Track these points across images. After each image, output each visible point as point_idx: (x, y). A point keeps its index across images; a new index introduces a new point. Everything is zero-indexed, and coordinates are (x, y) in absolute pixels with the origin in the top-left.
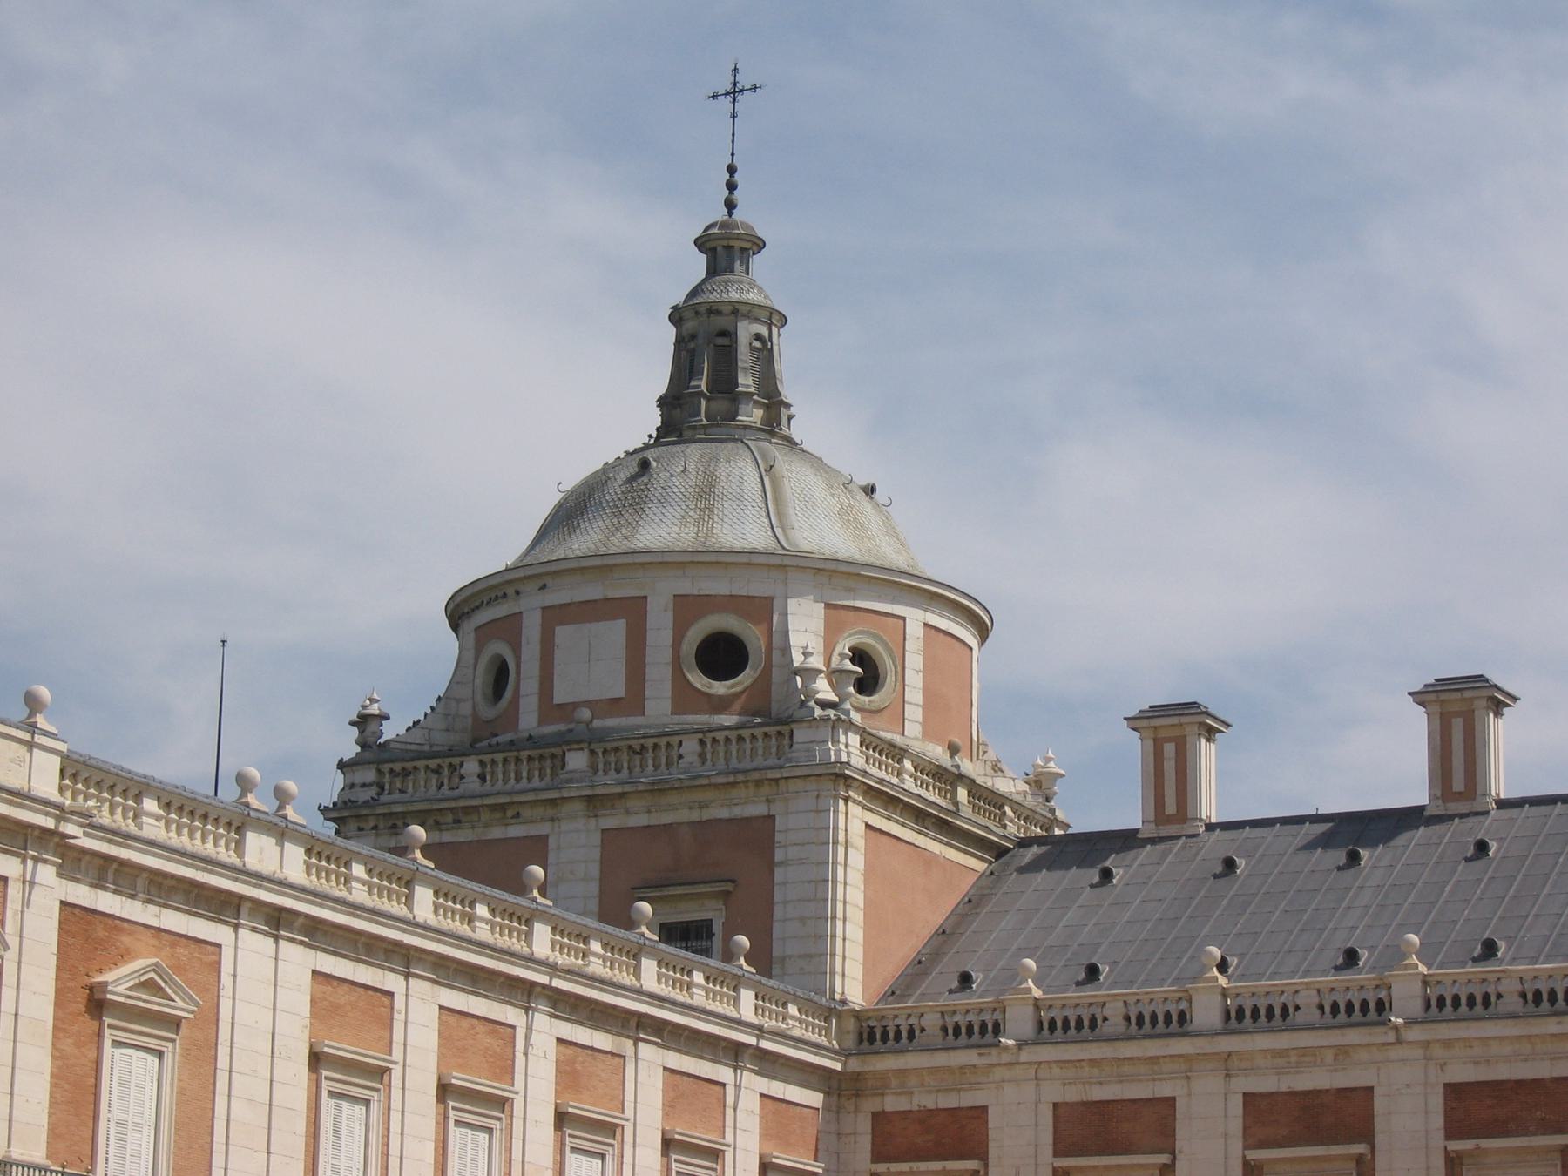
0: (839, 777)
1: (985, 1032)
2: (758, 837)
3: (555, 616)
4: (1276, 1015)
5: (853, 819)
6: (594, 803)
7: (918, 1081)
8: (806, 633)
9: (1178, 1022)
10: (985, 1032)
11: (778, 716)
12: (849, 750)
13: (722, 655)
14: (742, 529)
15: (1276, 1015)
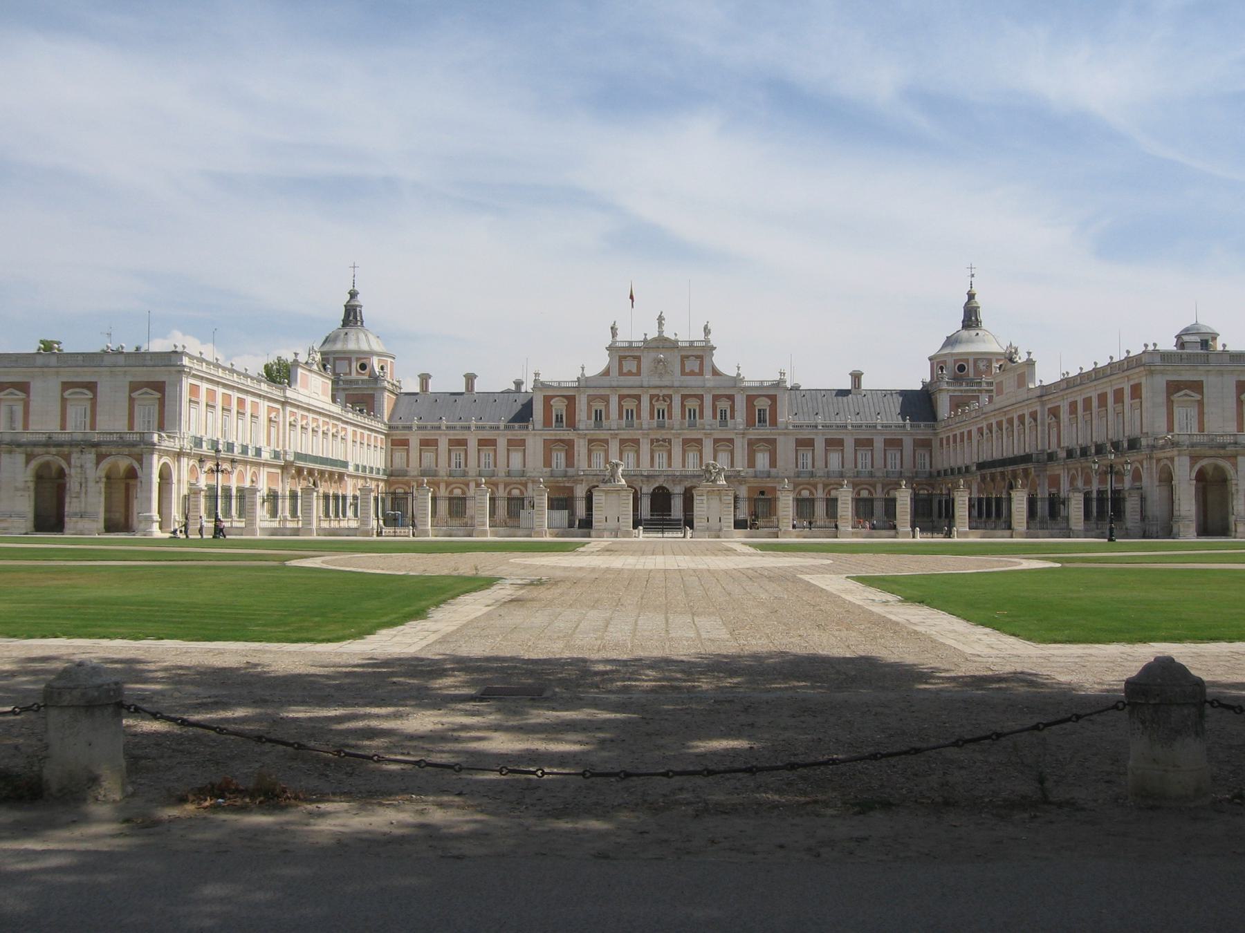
0: (385, 388)
1: (410, 428)
2: (372, 397)
3: (335, 359)
4: (453, 428)
5: (386, 394)
6: (344, 389)
7: (398, 435)
8: (375, 363)
9: (439, 428)
10: (410, 428)
11: (375, 379)
12: (386, 384)
13: (363, 367)
14: (365, 347)
15: (453, 428)
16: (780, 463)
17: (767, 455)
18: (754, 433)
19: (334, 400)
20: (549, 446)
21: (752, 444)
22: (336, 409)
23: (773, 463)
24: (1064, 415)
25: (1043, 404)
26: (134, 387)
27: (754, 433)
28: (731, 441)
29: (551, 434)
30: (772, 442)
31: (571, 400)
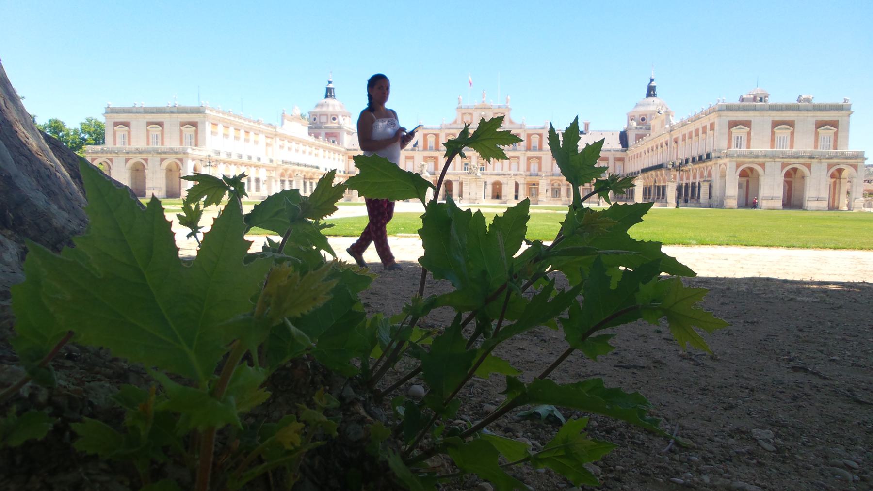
16: (543, 169)
17: (537, 165)
18: (530, 154)
19: (310, 134)
20: (426, 159)
21: (529, 158)
22: (312, 139)
23: (540, 169)
24: (680, 141)
25: (671, 136)
26: (183, 124)
27: (530, 154)
28: (518, 158)
29: (427, 153)
30: (539, 158)
31: (437, 136)
